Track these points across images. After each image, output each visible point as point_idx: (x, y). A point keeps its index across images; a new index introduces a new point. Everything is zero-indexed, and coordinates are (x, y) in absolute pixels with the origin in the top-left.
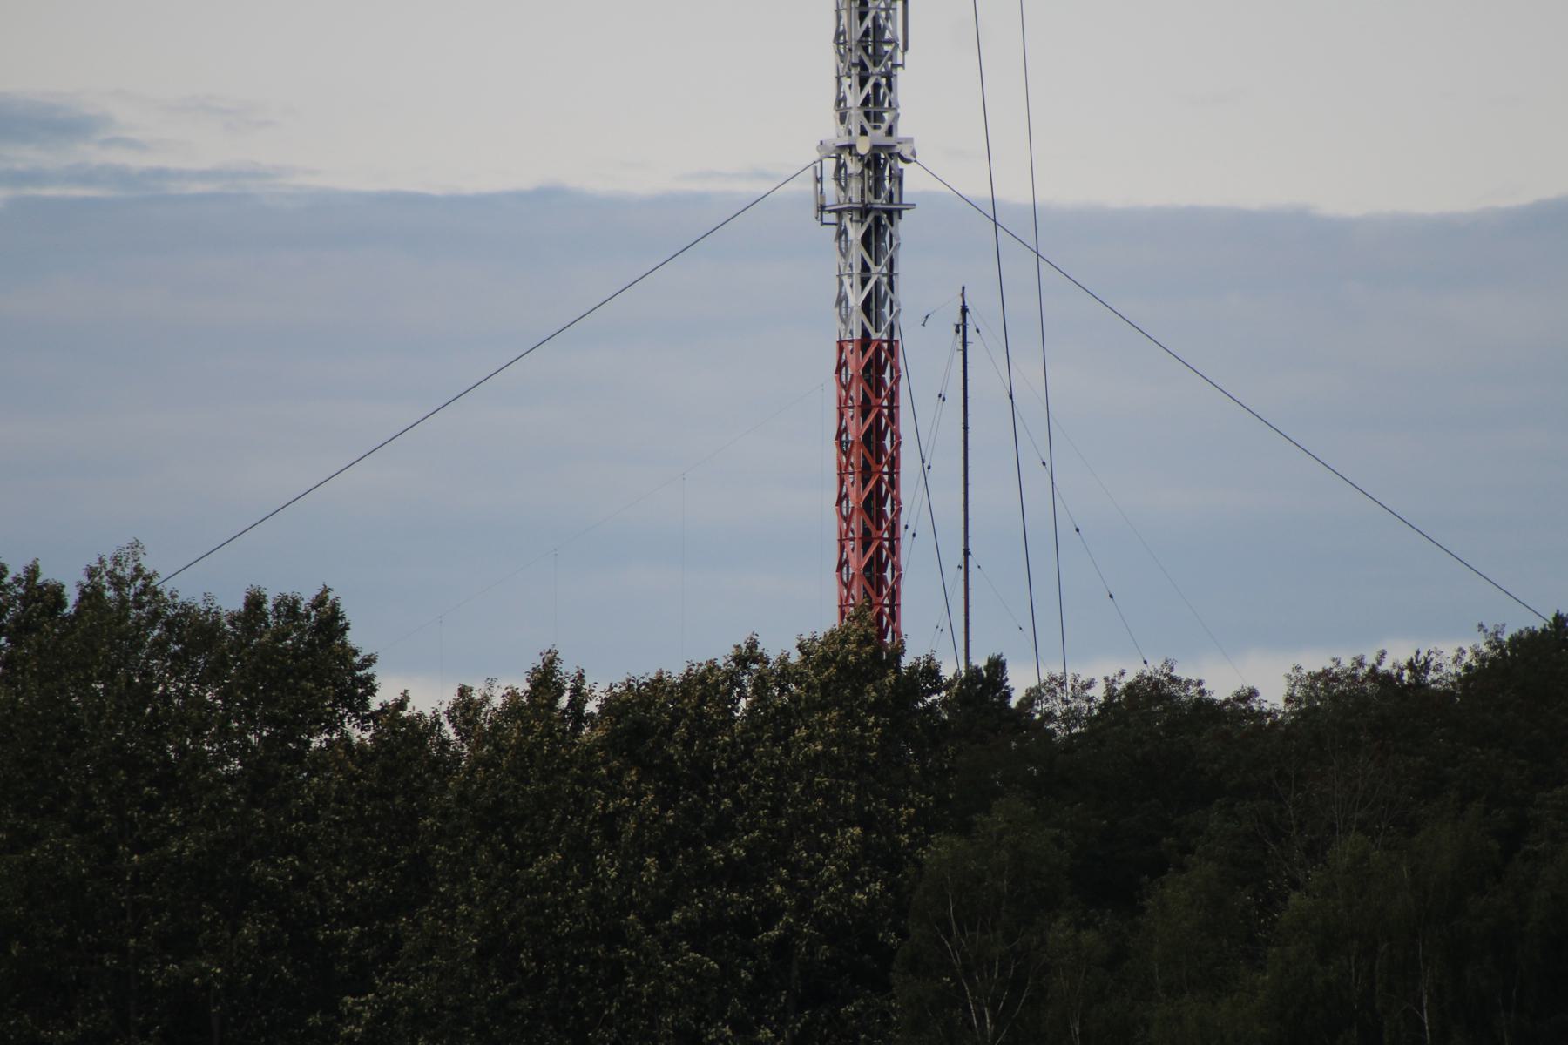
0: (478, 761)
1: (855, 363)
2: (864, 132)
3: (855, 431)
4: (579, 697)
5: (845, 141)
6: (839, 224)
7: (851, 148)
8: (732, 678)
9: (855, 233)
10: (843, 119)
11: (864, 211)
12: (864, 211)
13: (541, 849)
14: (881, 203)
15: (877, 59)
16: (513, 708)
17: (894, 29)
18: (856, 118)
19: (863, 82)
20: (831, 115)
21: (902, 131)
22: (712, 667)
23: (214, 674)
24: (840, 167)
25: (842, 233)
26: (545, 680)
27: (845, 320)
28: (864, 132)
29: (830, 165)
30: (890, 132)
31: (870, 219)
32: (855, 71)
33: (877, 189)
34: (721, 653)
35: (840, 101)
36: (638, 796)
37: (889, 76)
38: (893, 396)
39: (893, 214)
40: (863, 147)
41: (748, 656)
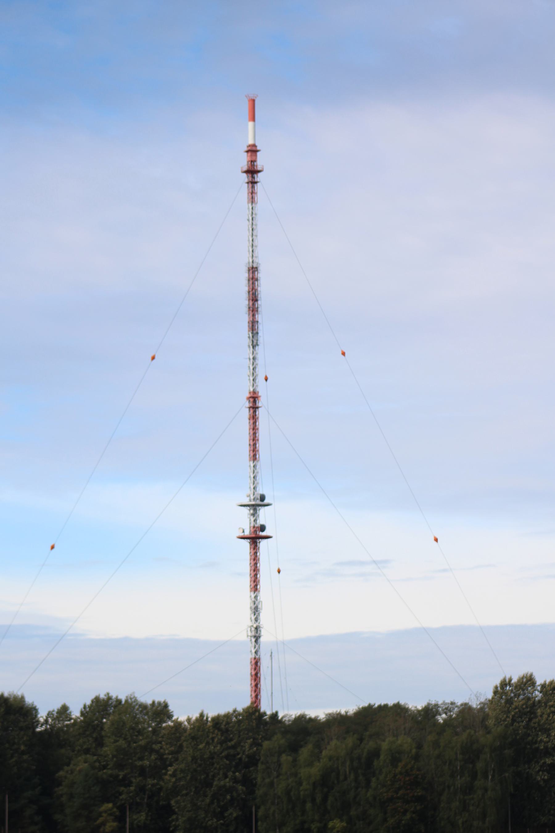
0: (191, 729)
1: (253, 662)
2: (255, 623)
3: (253, 673)
4: (207, 718)
5: (252, 625)
6: (251, 638)
7: (252, 626)
8: (232, 714)
9: (253, 640)
10: (251, 621)
11: (255, 637)
12: (255, 637)
13: (201, 743)
14: (257, 635)
15: (257, 611)
16: (197, 720)
17: (260, 606)
18: (253, 621)
19: (255, 615)
20: (249, 620)
21: (261, 623)
22: (229, 713)
23: (147, 714)
24: (251, 629)
25: (251, 640)
26: (202, 715)
27: (252, 654)
28: (255, 623)
29: (249, 629)
30: (259, 623)
31: (256, 638)
32: (253, 613)
33: (257, 632)
34: (231, 710)
35: (251, 618)
36: (217, 735)
37: (259, 614)
38: (260, 667)
39: (260, 637)
40: (255, 626)
41: (235, 711)
